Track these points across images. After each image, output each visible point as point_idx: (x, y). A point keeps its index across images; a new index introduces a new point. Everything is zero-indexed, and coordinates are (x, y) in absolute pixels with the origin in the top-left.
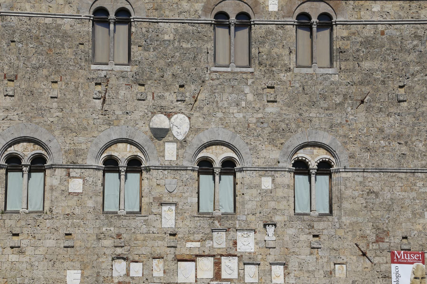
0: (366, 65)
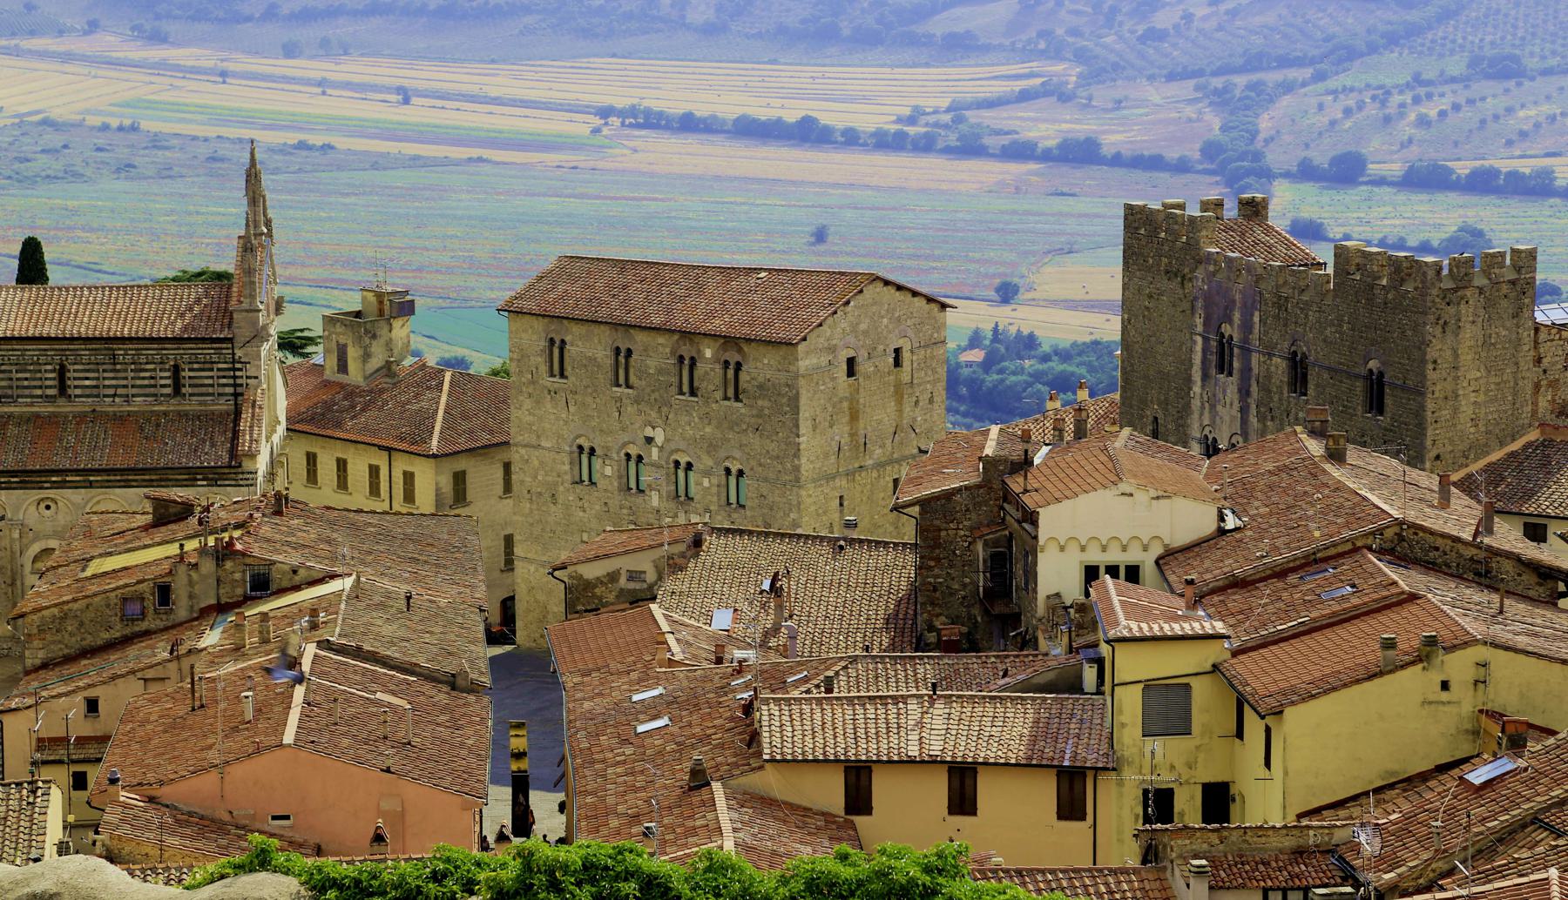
0: (760, 403)
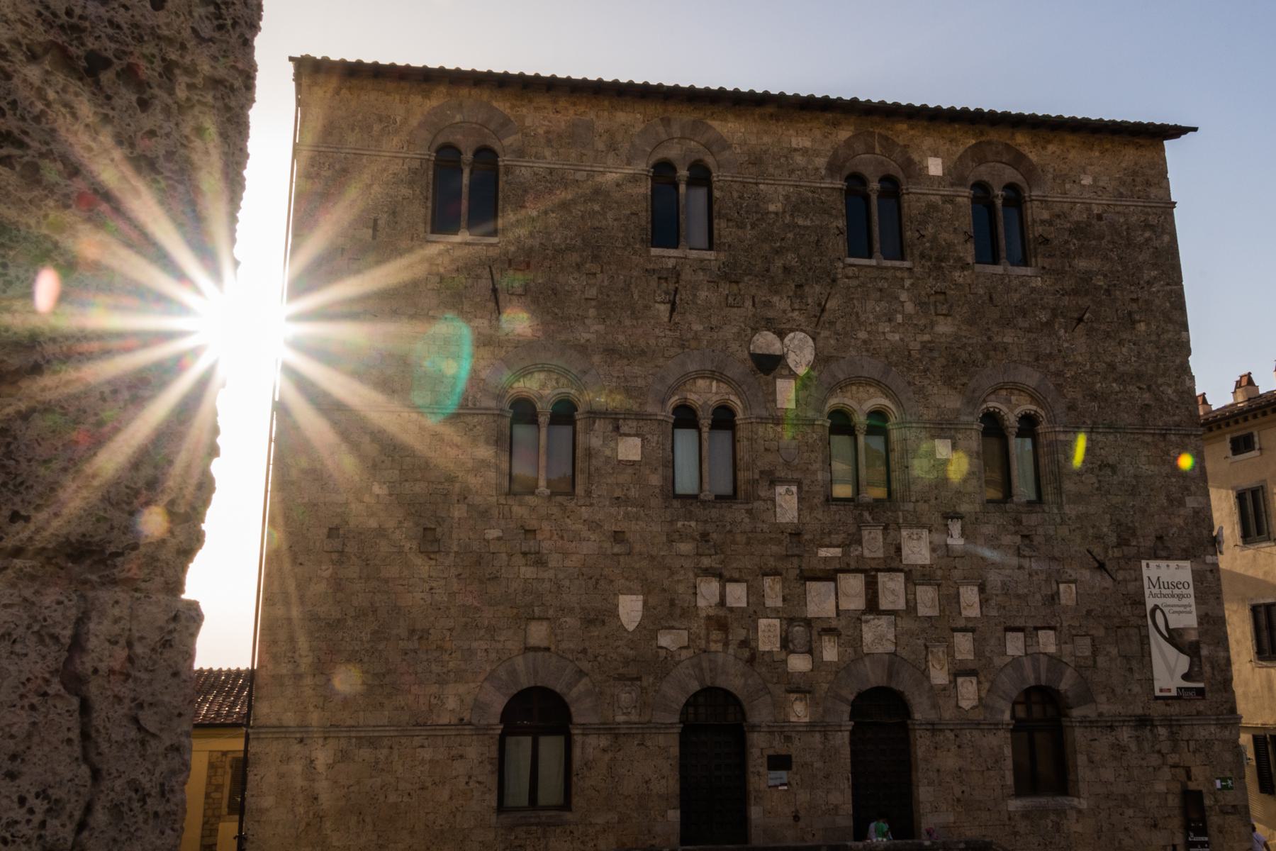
0: (1082, 264)
